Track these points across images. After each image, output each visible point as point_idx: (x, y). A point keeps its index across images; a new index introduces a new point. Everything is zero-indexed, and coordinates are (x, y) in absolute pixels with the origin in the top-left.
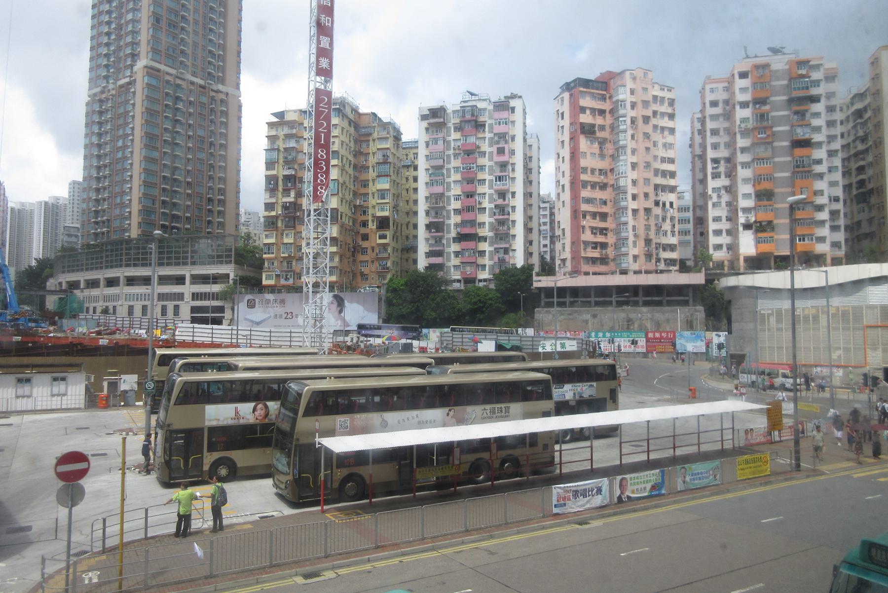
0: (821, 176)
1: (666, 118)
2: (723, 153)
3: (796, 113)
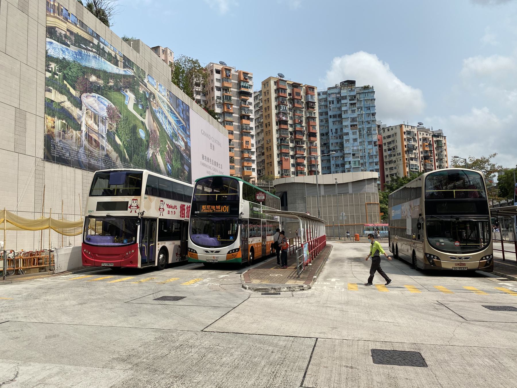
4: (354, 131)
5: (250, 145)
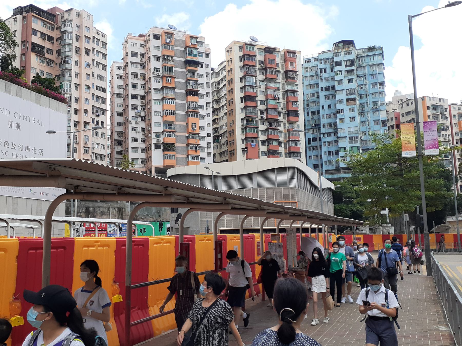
0: (203, 117)
1: (100, 55)
2: (140, 92)
3: (189, 71)
4: (351, 107)
5: (198, 127)
